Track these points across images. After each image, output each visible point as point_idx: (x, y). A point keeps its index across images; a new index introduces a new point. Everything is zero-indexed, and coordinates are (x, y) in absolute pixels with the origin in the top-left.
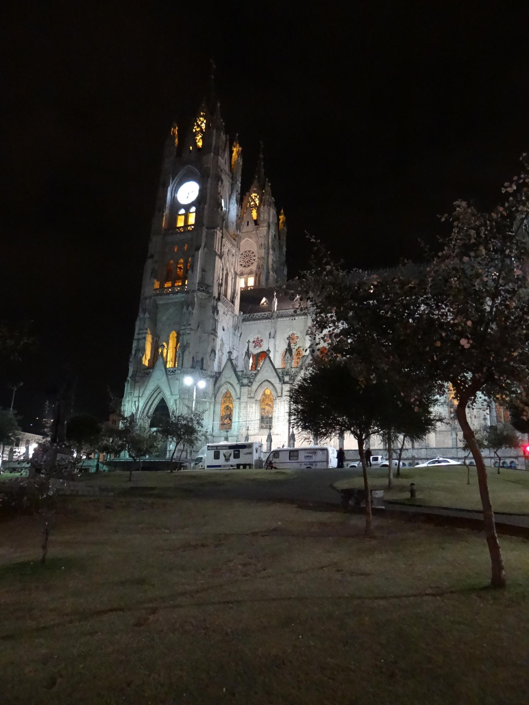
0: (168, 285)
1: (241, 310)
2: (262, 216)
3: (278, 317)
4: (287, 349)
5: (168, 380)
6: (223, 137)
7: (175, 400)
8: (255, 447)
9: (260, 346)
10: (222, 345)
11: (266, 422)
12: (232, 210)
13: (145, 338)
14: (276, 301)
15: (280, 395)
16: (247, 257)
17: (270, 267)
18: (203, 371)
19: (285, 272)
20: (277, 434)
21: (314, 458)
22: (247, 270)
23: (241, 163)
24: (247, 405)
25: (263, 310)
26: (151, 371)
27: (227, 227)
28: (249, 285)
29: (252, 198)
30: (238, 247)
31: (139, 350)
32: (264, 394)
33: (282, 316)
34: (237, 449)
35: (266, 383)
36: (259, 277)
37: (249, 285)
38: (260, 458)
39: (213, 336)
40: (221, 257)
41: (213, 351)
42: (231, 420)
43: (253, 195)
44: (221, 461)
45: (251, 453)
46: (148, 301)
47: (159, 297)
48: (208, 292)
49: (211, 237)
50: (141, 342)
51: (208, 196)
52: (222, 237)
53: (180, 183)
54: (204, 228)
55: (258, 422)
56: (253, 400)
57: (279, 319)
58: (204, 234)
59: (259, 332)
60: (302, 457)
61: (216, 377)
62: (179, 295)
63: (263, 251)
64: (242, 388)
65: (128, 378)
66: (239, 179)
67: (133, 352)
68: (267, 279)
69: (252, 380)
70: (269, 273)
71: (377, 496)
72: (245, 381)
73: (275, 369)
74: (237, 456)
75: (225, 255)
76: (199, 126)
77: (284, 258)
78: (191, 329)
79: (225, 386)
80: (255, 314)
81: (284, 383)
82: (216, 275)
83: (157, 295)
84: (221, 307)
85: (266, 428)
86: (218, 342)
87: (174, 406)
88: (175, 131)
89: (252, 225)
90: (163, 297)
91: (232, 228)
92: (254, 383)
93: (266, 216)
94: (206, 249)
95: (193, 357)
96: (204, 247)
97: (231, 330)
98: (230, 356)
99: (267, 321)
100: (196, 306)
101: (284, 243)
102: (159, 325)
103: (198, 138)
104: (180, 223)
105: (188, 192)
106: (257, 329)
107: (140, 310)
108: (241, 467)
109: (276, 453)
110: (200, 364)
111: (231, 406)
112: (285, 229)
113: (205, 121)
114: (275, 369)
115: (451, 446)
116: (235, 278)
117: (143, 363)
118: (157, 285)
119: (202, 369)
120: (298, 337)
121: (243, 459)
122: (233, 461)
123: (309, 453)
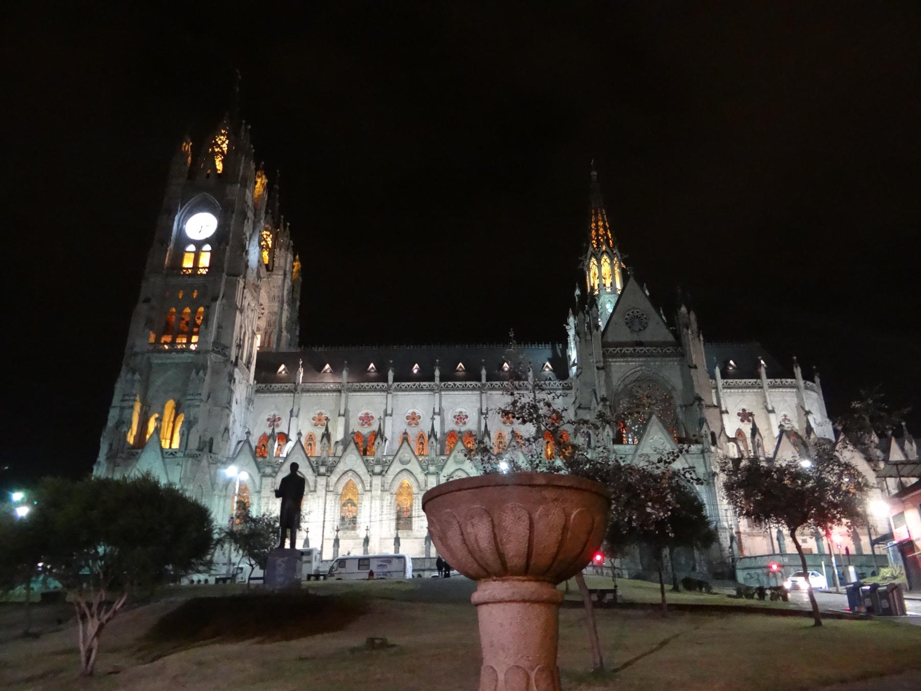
0: (167, 338)
1: (255, 378)
3: (303, 391)
5: (165, 465)
8: (315, 553)
10: (234, 421)
13: (132, 407)
17: (284, 325)
19: (297, 333)
21: (389, 568)
25: (280, 380)
26: (140, 451)
31: (124, 423)
33: (308, 391)
36: (270, 337)
39: (227, 410)
40: (241, 311)
41: (227, 429)
45: (309, 562)
46: (139, 358)
47: (157, 355)
48: (224, 355)
49: (232, 287)
50: (127, 411)
51: (231, 235)
52: (244, 288)
53: (191, 213)
57: (304, 394)
58: (224, 280)
59: (277, 408)
62: (186, 355)
63: (276, 306)
64: (264, 479)
66: (263, 216)
67: (111, 423)
76: (219, 146)
77: (296, 315)
78: (201, 401)
80: (273, 385)
81: (319, 475)
82: (235, 334)
83: (152, 352)
86: (231, 419)
88: (187, 147)
90: (162, 355)
91: (251, 276)
93: (282, 261)
94: (224, 301)
95: (200, 437)
97: (244, 403)
99: (288, 395)
100: (209, 371)
101: (298, 296)
102: (151, 393)
104: (188, 263)
105: (201, 225)
106: (276, 404)
107: (124, 368)
108: (322, 578)
109: (342, 562)
113: (227, 142)
117: (128, 439)
118: (152, 339)
119: (210, 451)
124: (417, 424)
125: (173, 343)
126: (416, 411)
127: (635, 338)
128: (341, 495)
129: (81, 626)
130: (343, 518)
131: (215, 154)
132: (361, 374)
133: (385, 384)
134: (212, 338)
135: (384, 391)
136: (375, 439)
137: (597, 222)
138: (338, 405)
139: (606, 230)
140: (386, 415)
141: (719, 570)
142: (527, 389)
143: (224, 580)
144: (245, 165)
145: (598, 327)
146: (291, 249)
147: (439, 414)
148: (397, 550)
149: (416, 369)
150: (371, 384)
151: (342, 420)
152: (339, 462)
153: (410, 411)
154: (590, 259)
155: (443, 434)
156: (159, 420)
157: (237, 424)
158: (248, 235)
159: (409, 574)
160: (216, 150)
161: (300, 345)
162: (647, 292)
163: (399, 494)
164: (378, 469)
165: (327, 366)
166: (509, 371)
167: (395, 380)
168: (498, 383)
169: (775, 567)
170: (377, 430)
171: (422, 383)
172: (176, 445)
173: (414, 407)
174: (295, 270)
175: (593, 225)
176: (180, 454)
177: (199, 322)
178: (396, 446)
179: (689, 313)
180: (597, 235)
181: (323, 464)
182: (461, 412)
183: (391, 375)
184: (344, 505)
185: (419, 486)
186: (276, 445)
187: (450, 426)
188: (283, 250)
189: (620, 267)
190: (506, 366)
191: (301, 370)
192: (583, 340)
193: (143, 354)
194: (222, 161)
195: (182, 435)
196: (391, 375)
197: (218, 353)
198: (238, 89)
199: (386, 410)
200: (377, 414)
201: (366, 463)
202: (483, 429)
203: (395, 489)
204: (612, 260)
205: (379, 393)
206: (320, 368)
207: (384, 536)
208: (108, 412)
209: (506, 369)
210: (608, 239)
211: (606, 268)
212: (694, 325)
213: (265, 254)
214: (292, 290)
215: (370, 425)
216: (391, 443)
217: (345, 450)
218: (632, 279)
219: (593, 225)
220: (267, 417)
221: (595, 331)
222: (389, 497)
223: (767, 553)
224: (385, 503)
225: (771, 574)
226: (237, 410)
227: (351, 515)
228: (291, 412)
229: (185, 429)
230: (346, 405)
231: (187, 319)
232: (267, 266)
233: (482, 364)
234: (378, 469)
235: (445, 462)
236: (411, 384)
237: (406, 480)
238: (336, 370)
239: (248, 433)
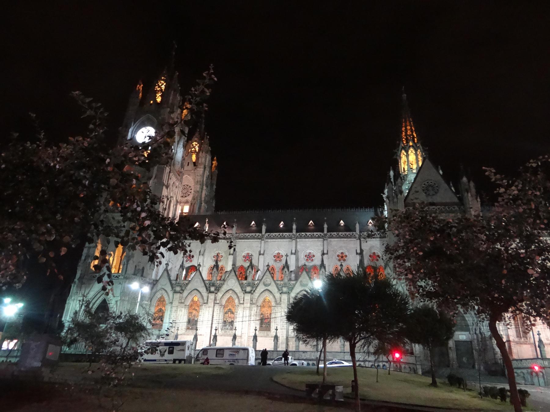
2: (200, 160)
4: (214, 265)
6: (179, 98)
7: (117, 301)
9: (191, 261)
11: (192, 323)
12: (179, 152)
15: (206, 302)
16: (186, 190)
17: (203, 199)
18: (144, 279)
19: (214, 205)
20: (201, 335)
21: (237, 356)
22: (184, 199)
24: (177, 308)
27: (174, 165)
28: (184, 211)
29: (193, 145)
30: (181, 181)
31: (89, 256)
32: (193, 300)
34: (172, 346)
35: (195, 291)
36: (194, 206)
37: (184, 211)
38: (190, 354)
40: (167, 187)
42: (162, 321)
43: (194, 143)
44: (156, 356)
45: (184, 350)
50: (91, 250)
52: (170, 172)
53: (139, 128)
55: (186, 324)
56: (183, 305)
60: (226, 355)
61: (154, 284)
63: (198, 187)
64: (175, 294)
65: (76, 280)
67: (83, 258)
68: (200, 208)
69: (183, 288)
70: (201, 203)
71: (338, 391)
72: (178, 289)
73: (204, 281)
74: (171, 352)
75: (171, 186)
76: (159, 87)
79: (160, 292)
85: (192, 329)
87: (115, 306)
88: (140, 87)
89: (191, 165)
91: (178, 167)
92: (185, 292)
93: (203, 160)
94: (155, 180)
95: (136, 266)
98: (167, 267)
101: (215, 182)
103: (158, 95)
110: (141, 272)
111: (163, 309)
112: (217, 171)
113: (165, 84)
114: (204, 281)
115: (340, 351)
116: (176, 205)
119: (142, 276)
120: (222, 256)
121: (177, 355)
122: (167, 356)
123: (234, 352)
126: (280, 252)
127: (430, 200)
128: (224, 307)
130: (225, 322)
131: (156, 92)
133: (260, 234)
135: (259, 239)
137: (406, 127)
139: (412, 132)
141: (493, 369)
142: (355, 238)
145: (401, 192)
146: (209, 153)
147: (295, 254)
149: (281, 225)
150: (251, 234)
151: (231, 257)
152: (223, 284)
153: (276, 252)
154: (401, 151)
155: (297, 267)
160: (158, 89)
162: (441, 172)
163: (262, 306)
164: (248, 289)
166: (344, 225)
167: (266, 232)
168: (335, 233)
169: (537, 368)
171: (284, 234)
173: (279, 249)
175: (404, 129)
179: (469, 182)
180: (406, 135)
181: (213, 285)
182: (310, 253)
183: (264, 228)
184: (226, 313)
185: (276, 301)
187: (302, 262)
189: (422, 156)
192: (392, 202)
196: (264, 228)
198: (174, 53)
199: (260, 252)
201: (242, 285)
203: (260, 303)
204: (416, 151)
205: (256, 240)
208: (83, 250)
210: (414, 138)
211: (412, 157)
212: (473, 190)
218: (427, 160)
219: (404, 129)
221: (399, 195)
222: (255, 309)
223: (532, 357)
225: (534, 374)
227: (230, 320)
233: (325, 221)
234: (248, 289)
235: (294, 285)
236: (277, 234)
237: (270, 297)
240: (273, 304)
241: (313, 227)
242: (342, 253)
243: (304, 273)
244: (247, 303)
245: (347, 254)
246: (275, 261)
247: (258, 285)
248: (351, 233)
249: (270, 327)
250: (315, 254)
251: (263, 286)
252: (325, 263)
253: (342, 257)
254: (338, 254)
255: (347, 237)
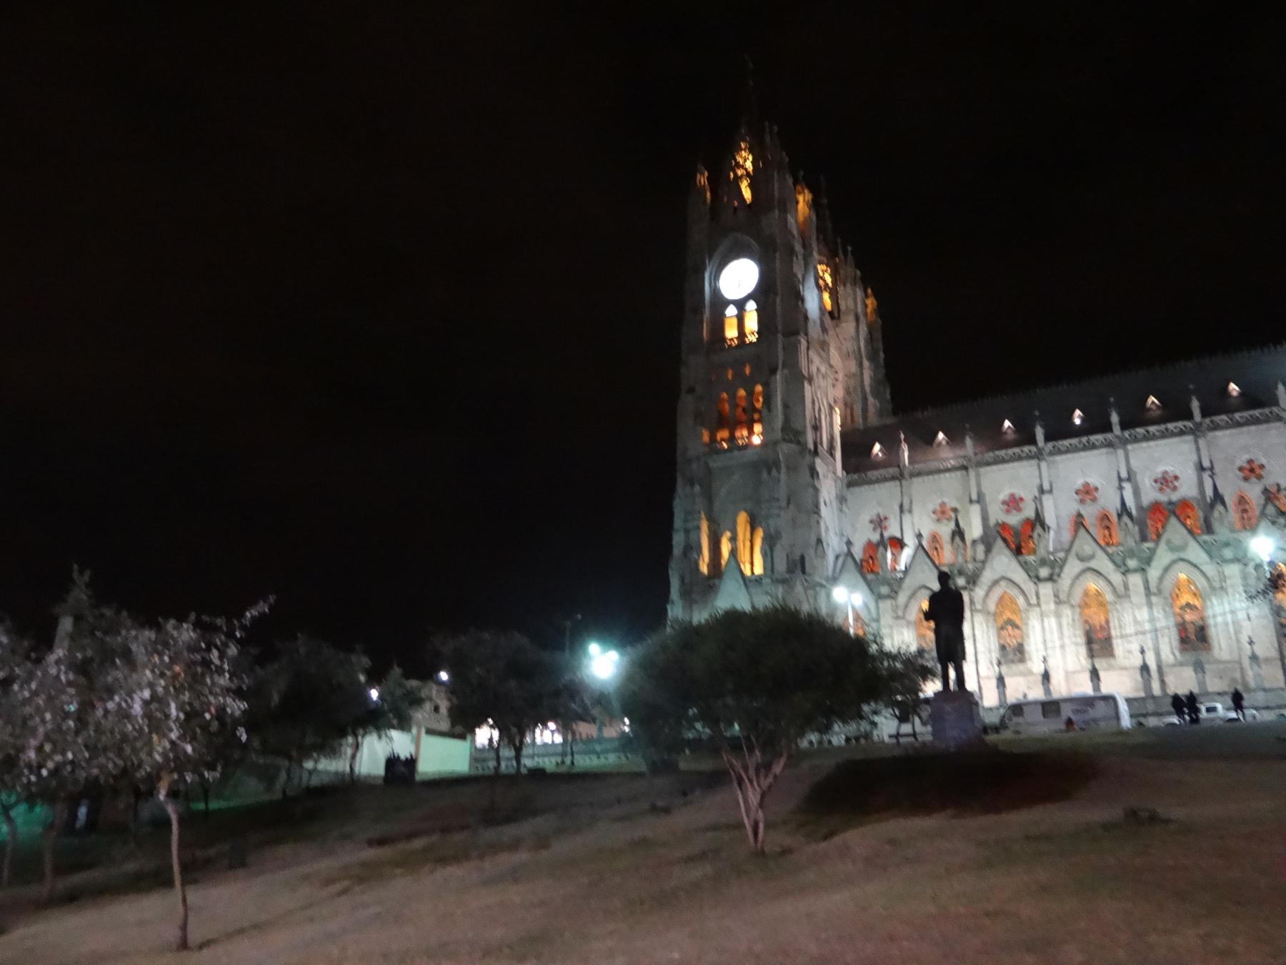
0: (724, 434)
1: (844, 467)
3: (913, 475)
10: (827, 529)
13: (698, 528)
14: (905, 449)
17: (868, 389)
19: (888, 397)
21: (1092, 713)
23: (814, 218)
25: (877, 465)
26: (717, 581)
33: (919, 474)
36: (852, 409)
41: (819, 541)
46: (694, 466)
48: (798, 443)
49: (792, 351)
50: (693, 536)
52: (808, 348)
54: (780, 336)
57: (915, 480)
59: (880, 504)
63: (853, 367)
67: (677, 551)
68: (865, 410)
78: (780, 508)
84: (820, 466)
88: (702, 179)
91: (814, 330)
93: (850, 303)
94: (786, 371)
96: (784, 366)
97: (835, 503)
100: (783, 470)
101: (880, 345)
102: (717, 505)
104: (731, 332)
105: (739, 277)
106: (878, 498)
109: (1017, 709)
112: (880, 321)
113: (751, 158)
118: (706, 438)
119: (804, 572)
124: (1094, 500)
125: (732, 439)
128: (995, 614)
129: (739, 793)
130: (1003, 648)
131: (738, 179)
132: (992, 440)
134: (779, 423)
136: (1033, 530)
138: (966, 488)
140: (1042, 491)
143: (857, 739)
144: (780, 182)
147: (1129, 479)
148: (1096, 687)
150: (1010, 451)
152: (983, 568)
153: (1079, 483)
155: (1140, 508)
156: (733, 539)
157: (831, 533)
158: (800, 277)
159: (1126, 722)
161: (895, 413)
163: (1084, 605)
164: (1044, 572)
165: (941, 436)
166: (1241, 394)
167: (1048, 438)
168: (1224, 417)
170: (1032, 515)
171: (1093, 438)
172: (759, 570)
174: (869, 310)
176: (766, 581)
177: (759, 405)
178: (1066, 536)
181: (961, 573)
182: (1166, 472)
183: (1039, 433)
186: (889, 555)
187: (1150, 494)
188: (848, 285)
190: (1234, 388)
191: (905, 447)
193: (698, 458)
194: (750, 186)
195: (764, 555)
196: (1039, 433)
197: (791, 441)
200: (1028, 494)
201: (1025, 566)
202: (1209, 492)
203: (1077, 597)
206: (930, 440)
207: (1071, 667)
208: (670, 539)
209: (1235, 394)
213: (826, 296)
214: (871, 338)
215: (1019, 510)
216: (1058, 532)
217: (988, 550)
220: (868, 518)
224: (1064, 621)
226: (828, 513)
227: (1014, 642)
228: (901, 507)
229: (767, 548)
230: (979, 486)
231: (743, 404)
232: (831, 313)
234: (1044, 572)
236: (1074, 441)
237: (1093, 584)
238: (955, 438)
239: (849, 543)
240: (1109, 597)
241: (1158, 412)
242: (1250, 462)
243: (1173, 520)
244: (1047, 603)
245: (1263, 461)
246: (1082, 501)
247: (1064, 561)
248: (1267, 411)
249: (1112, 649)
250: (1178, 473)
251: (1077, 562)
252: (1220, 490)
253: (1252, 470)
254: (1239, 463)
255: (1256, 421)
